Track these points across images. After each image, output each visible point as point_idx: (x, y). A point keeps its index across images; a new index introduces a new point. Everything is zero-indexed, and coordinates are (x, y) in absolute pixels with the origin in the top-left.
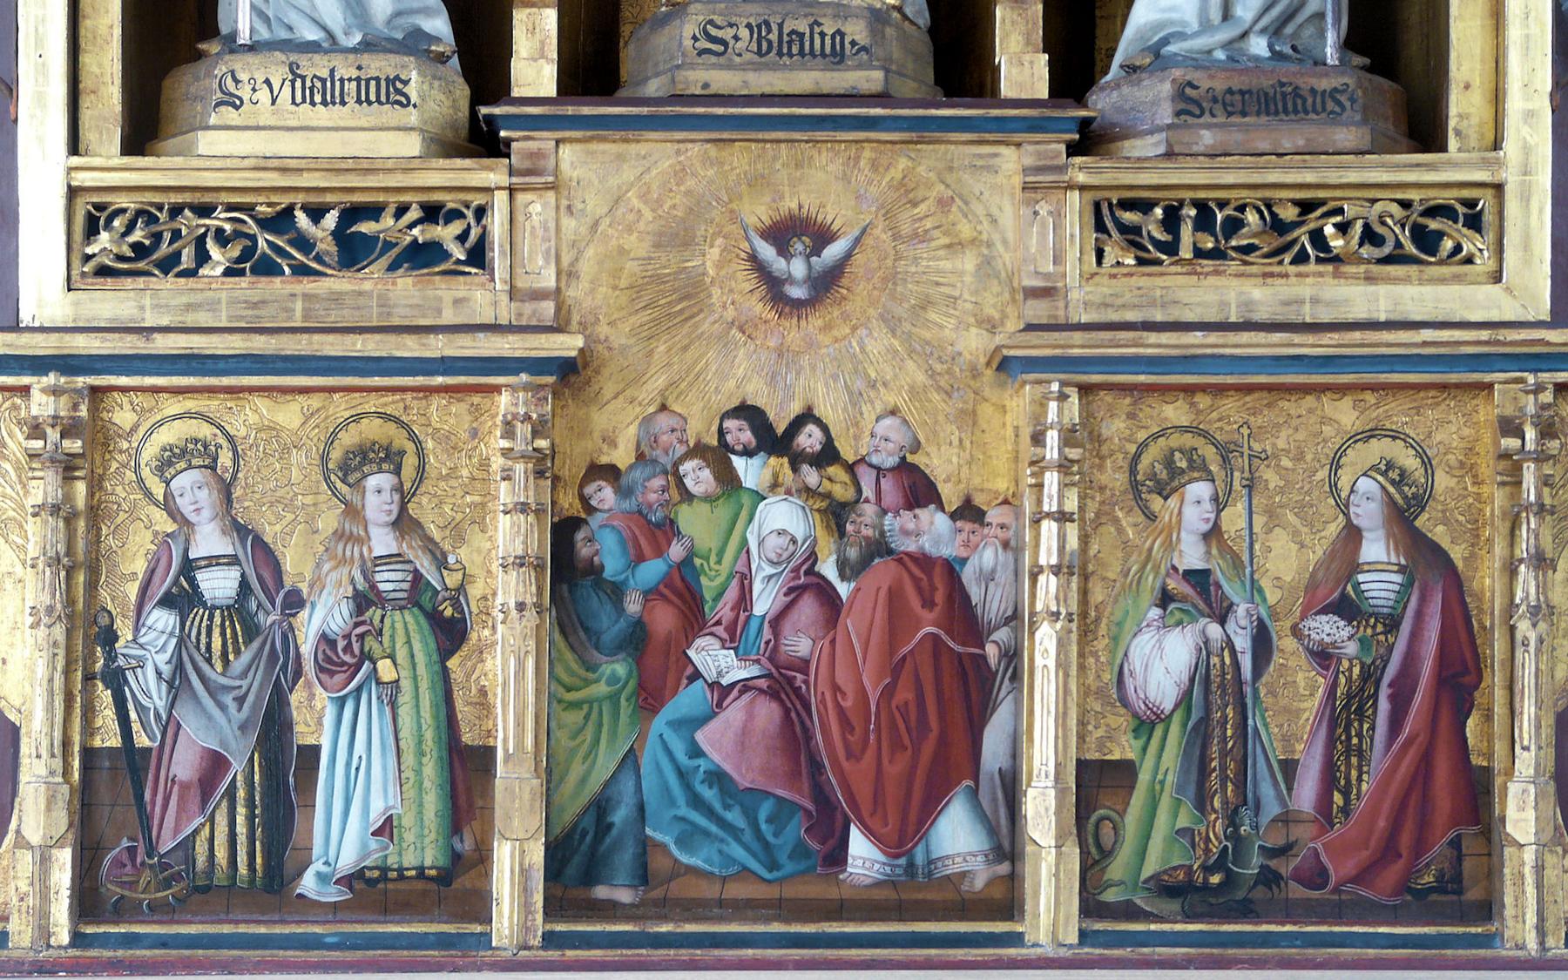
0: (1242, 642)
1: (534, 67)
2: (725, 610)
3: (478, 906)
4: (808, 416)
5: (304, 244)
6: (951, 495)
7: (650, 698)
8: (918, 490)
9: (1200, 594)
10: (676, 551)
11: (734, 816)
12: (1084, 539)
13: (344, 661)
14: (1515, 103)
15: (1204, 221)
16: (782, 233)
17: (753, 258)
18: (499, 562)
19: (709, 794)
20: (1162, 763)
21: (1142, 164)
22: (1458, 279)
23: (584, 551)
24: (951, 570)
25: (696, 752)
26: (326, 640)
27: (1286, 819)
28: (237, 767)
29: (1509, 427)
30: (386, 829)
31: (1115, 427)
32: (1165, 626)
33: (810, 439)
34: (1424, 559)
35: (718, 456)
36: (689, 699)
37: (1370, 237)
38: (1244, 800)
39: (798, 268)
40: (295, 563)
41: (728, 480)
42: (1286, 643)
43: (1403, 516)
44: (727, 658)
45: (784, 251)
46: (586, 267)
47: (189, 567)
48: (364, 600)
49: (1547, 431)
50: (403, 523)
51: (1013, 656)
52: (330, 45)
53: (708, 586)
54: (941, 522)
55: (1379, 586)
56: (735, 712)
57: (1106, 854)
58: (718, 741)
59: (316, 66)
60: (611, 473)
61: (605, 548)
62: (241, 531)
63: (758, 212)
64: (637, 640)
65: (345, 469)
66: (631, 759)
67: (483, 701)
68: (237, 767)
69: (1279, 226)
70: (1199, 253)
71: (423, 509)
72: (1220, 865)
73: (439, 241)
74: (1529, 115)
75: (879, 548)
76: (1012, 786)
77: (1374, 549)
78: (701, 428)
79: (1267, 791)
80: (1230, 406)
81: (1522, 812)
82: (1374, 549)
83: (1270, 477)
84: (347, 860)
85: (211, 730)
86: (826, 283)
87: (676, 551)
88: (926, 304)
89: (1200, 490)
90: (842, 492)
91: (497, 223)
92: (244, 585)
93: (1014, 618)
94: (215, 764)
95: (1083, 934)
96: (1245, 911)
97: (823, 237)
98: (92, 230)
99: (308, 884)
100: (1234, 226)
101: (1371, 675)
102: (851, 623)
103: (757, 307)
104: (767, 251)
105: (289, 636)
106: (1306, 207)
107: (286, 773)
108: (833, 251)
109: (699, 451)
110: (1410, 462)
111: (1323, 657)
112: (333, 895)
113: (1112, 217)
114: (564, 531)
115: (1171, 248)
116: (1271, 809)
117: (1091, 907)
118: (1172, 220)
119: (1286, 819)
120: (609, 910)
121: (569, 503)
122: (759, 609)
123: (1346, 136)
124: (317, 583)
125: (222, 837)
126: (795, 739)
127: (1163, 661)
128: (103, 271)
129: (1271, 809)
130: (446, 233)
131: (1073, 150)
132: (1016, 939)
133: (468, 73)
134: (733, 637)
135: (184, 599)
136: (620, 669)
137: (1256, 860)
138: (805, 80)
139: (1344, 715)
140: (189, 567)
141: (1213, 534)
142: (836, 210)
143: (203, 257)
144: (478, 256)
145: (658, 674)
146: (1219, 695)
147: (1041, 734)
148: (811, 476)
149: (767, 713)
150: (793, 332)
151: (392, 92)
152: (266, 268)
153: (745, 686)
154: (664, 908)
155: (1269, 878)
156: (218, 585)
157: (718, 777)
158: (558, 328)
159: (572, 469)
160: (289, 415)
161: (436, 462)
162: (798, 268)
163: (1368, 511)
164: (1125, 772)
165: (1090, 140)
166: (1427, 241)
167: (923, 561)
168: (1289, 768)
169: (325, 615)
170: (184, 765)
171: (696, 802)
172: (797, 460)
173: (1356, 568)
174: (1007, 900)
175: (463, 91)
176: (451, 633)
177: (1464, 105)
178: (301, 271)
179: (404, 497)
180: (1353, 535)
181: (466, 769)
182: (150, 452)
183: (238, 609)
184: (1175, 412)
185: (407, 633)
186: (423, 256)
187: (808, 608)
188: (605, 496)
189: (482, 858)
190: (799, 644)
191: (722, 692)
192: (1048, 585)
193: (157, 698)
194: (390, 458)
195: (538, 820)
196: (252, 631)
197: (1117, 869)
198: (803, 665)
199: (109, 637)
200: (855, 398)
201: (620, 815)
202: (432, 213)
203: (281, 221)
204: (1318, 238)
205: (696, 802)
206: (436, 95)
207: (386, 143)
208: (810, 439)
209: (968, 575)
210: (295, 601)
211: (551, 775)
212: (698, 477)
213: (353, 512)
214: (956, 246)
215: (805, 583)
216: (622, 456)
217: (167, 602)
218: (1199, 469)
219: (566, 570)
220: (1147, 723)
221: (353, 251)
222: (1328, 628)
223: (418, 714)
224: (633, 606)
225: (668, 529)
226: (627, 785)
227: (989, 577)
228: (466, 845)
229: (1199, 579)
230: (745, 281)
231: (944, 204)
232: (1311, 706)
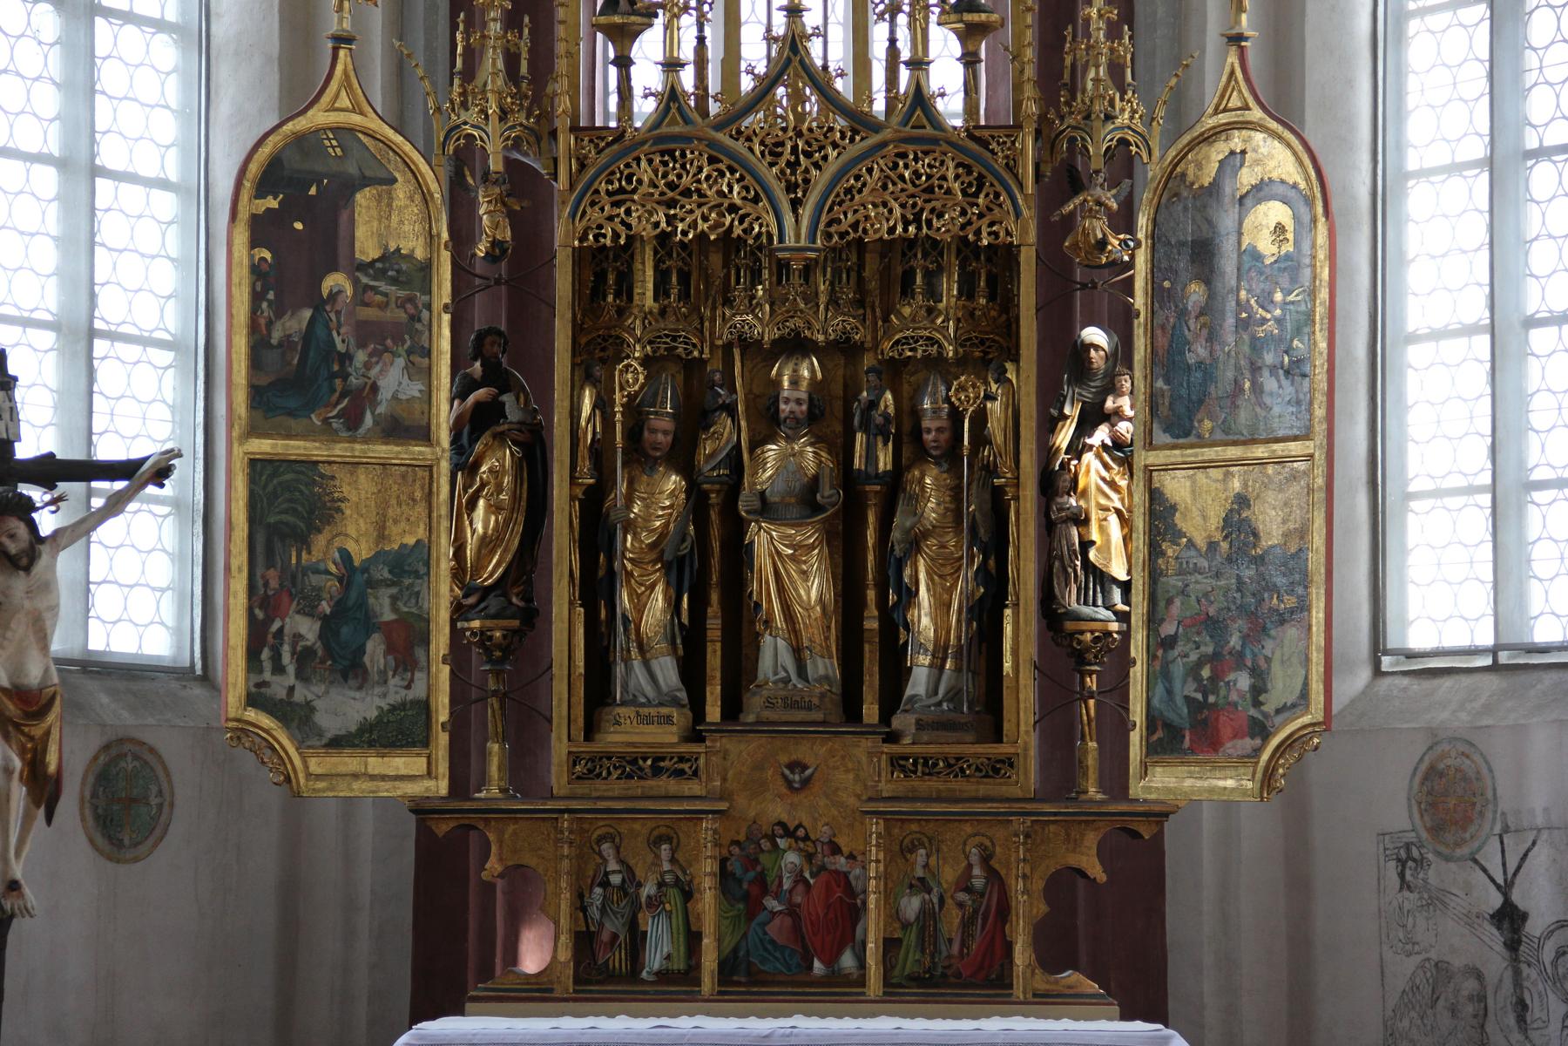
0: (935, 900)
1: (714, 712)
2: (774, 887)
3: (697, 982)
4: (800, 825)
5: (641, 769)
6: (845, 850)
7: (751, 916)
8: (835, 849)
9: (922, 885)
10: (759, 868)
11: (778, 954)
12: (886, 867)
13: (654, 903)
14: (1022, 728)
15: (925, 764)
16: (792, 766)
17: (783, 774)
18: (705, 873)
19: (770, 947)
20: (912, 937)
21: (906, 746)
22: (1005, 784)
23: (730, 868)
24: (846, 875)
25: (765, 933)
26: (649, 897)
27: (949, 957)
28: (622, 937)
29: (1017, 835)
30: (668, 958)
31: (896, 831)
32: (911, 895)
33: (801, 832)
34: (992, 875)
35: (772, 838)
36: (762, 917)
37: (978, 769)
38: (936, 951)
39: (797, 778)
40: (639, 873)
41: (775, 845)
42: (949, 901)
43: (986, 860)
44: (775, 903)
45: (793, 772)
46: (730, 774)
47: (607, 874)
48: (661, 885)
49: (1027, 836)
50: (673, 860)
51: (864, 903)
52: (649, 703)
53: (769, 879)
54: (843, 860)
55: (978, 883)
56: (777, 921)
57: (893, 967)
58: (773, 929)
59: (645, 711)
60: (737, 843)
61: (735, 866)
62: (621, 862)
63: (784, 759)
64: (746, 897)
65: (655, 843)
66: (745, 935)
67: (698, 917)
68: (622, 937)
69: (949, 766)
70: (924, 774)
71: (679, 856)
72: (929, 971)
73: (683, 768)
74: (1027, 732)
75: (823, 868)
76: (864, 944)
77: (977, 871)
78: (766, 829)
79: (943, 948)
80: (931, 825)
81: (1022, 955)
82: (977, 871)
83: (945, 848)
84: (656, 966)
85: (613, 926)
86: (806, 782)
87: (759, 868)
88: (837, 789)
89: (922, 851)
90: (811, 850)
91: (702, 761)
92: (624, 880)
93: (864, 892)
94: (615, 936)
95: (885, 993)
96: (937, 986)
97: (805, 767)
98: (575, 765)
99: (644, 974)
100: (935, 765)
101: (976, 911)
102: (814, 892)
103: (784, 790)
104: (787, 772)
105: (638, 896)
106: (958, 759)
107: (637, 940)
108: (808, 772)
109: (765, 836)
110: (988, 843)
111: (961, 905)
112: (652, 978)
113: (896, 762)
114: (723, 862)
115: (915, 772)
116: (945, 954)
117: (887, 982)
118: (915, 764)
119: (949, 957)
120: (739, 984)
121: (725, 852)
122: (785, 887)
123: (969, 737)
124: (646, 879)
125: (618, 959)
126: (796, 929)
127: (911, 906)
128: (579, 778)
129: (945, 954)
130: (686, 766)
131: (884, 741)
132: (863, 994)
133: (692, 709)
134: (777, 897)
135: (605, 884)
136: (741, 906)
137: (940, 970)
138: (800, 715)
139: (967, 924)
140: (607, 874)
141: (926, 866)
142: (809, 759)
143: (609, 773)
144: (695, 773)
145: (753, 907)
146: (928, 916)
147: (873, 931)
148: (801, 845)
149: (788, 921)
150: (796, 798)
151: (668, 720)
152: (629, 777)
153: (781, 912)
154: (755, 984)
155: (944, 975)
156: (616, 879)
157: (773, 942)
158: (721, 799)
159: (726, 842)
160: (637, 826)
161: (683, 839)
162: (797, 778)
163: (974, 859)
164: (899, 941)
165: (893, 737)
166: (997, 771)
167: (837, 872)
168: (950, 941)
169: (649, 889)
170: (605, 937)
171: (766, 949)
172: (797, 839)
173: (970, 877)
174: (862, 982)
175: (689, 714)
176: (688, 894)
177: (1007, 727)
178: (640, 778)
179: (673, 851)
180: (970, 866)
181: (693, 939)
182: (595, 836)
183: (622, 887)
184: (914, 827)
185: (674, 894)
186: (681, 773)
187: (800, 888)
188: (736, 850)
189: (698, 966)
190: (798, 899)
191: (774, 914)
192: (873, 882)
193: (597, 916)
194: (669, 840)
195: (715, 955)
196: (626, 894)
197: (896, 972)
198: (799, 906)
199: (581, 896)
200: (815, 820)
201: (741, 953)
202: (681, 759)
203: (634, 762)
204: (962, 770)
205: (766, 949)
206: (681, 717)
207: (667, 736)
208: (801, 832)
209: (851, 877)
210: (640, 885)
211: (719, 940)
212: (765, 844)
213: (658, 856)
214: (847, 771)
215: (800, 879)
216: (742, 838)
217: (600, 885)
218: (922, 845)
219: (725, 876)
220: (906, 926)
221: (657, 771)
222: (962, 896)
223: (678, 920)
224: (745, 886)
225: (757, 861)
226: (743, 943)
227: (857, 878)
228: (693, 963)
229: (922, 880)
230: (780, 781)
231: (843, 757)
232: (957, 921)
